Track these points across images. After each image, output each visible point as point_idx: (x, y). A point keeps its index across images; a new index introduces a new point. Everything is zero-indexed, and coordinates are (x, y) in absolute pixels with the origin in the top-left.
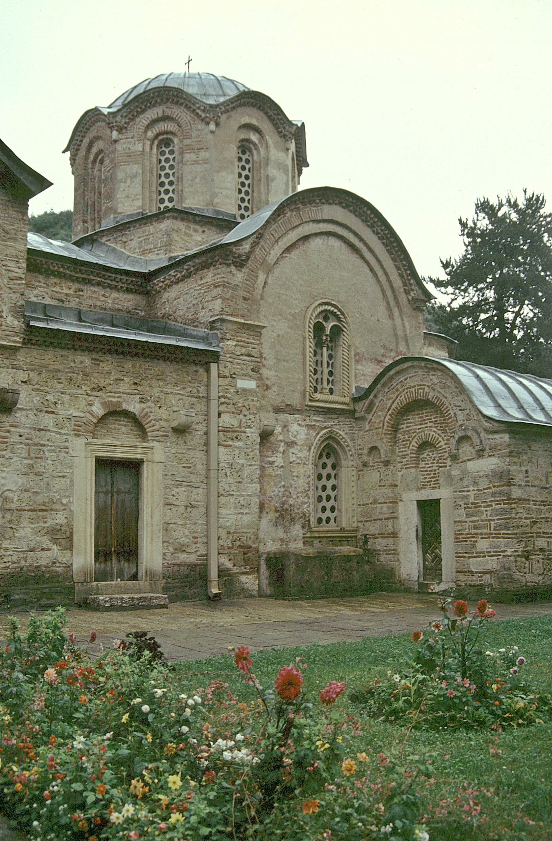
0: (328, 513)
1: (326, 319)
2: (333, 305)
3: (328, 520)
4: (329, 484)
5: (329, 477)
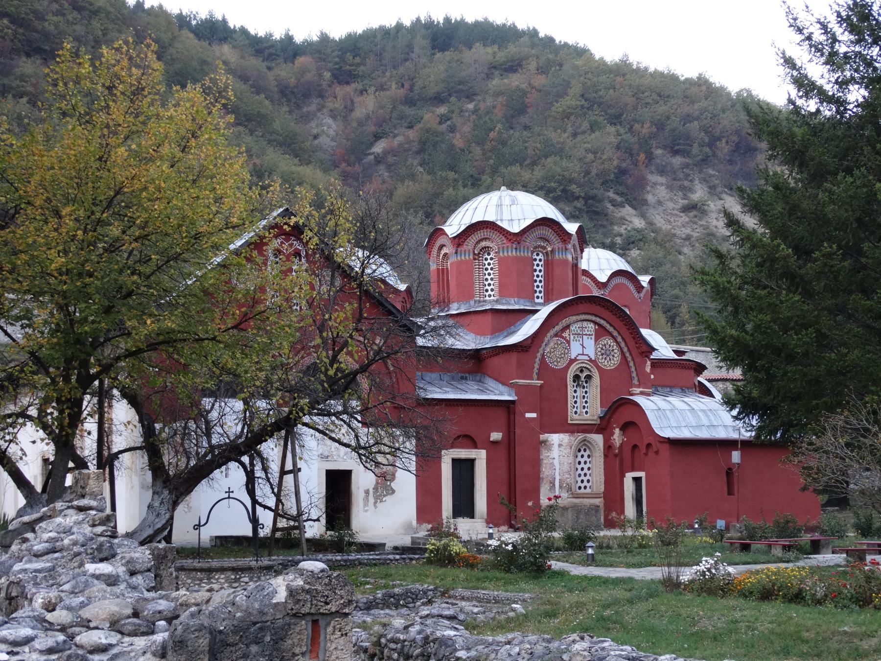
0: (585, 483)
1: (582, 371)
3: (585, 487)
5: (585, 463)
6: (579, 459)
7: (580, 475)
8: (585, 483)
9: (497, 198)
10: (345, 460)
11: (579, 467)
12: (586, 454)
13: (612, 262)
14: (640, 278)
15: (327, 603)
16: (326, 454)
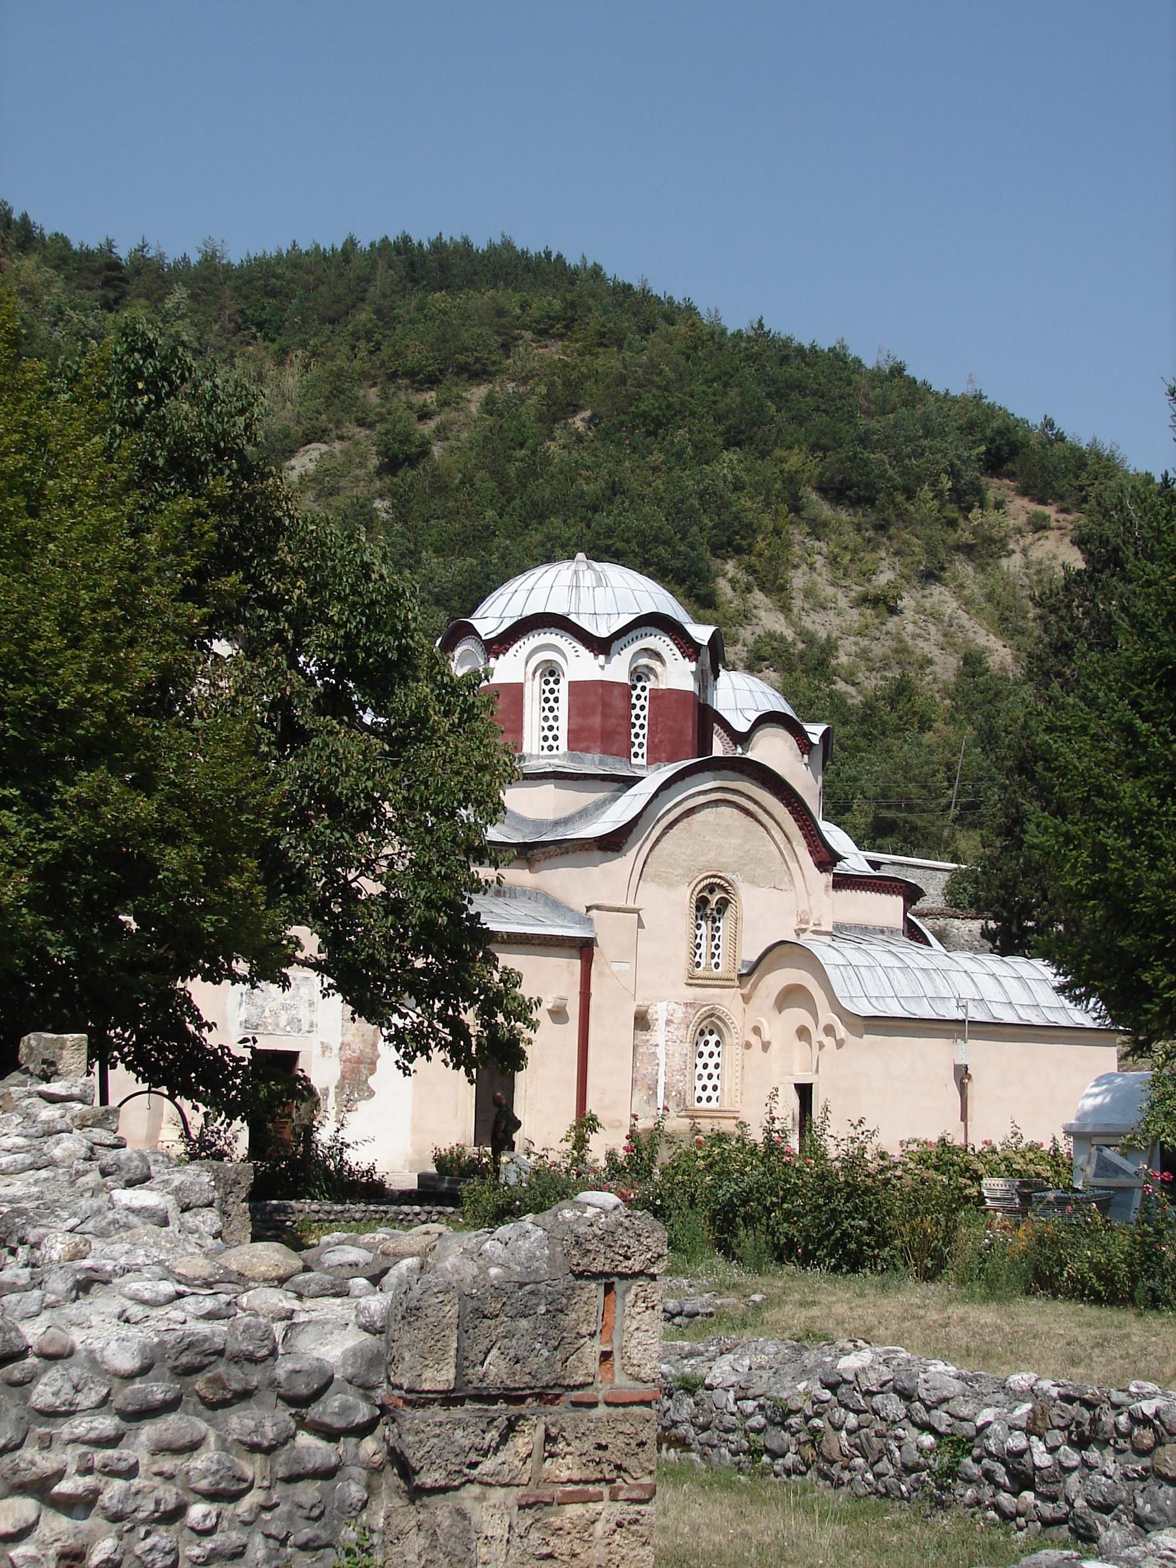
0: (709, 1092)
1: (712, 891)
2: (720, 877)
3: (709, 1099)
4: (711, 1062)
5: (711, 1055)
6: (702, 1048)
7: (700, 1077)
8: (709, 1092)
9: (570, 572)
10: (288, 1034)
11: (700, 1062)
12: (713, 1039)
13: (759, 696)
14: (808, 728)
15: (627, 1258)
16: (255, 1020)
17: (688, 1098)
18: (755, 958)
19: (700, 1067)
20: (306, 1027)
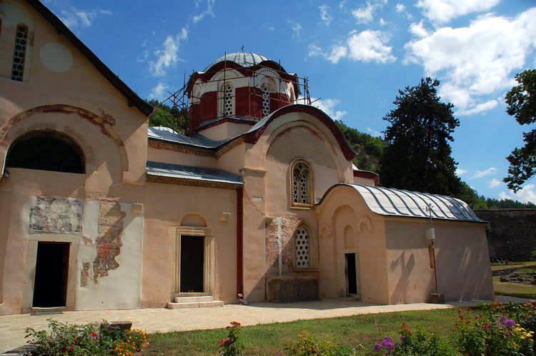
1: (300, 167)
3: (304, 263)
6: (299, 239)
10: (62, 232)
11: (299, 246)
12: (305, 234)
16: (41, 225)
17: (294, 263)
18: (321, 197)
19: (299, 248)
20: (74, 228)
